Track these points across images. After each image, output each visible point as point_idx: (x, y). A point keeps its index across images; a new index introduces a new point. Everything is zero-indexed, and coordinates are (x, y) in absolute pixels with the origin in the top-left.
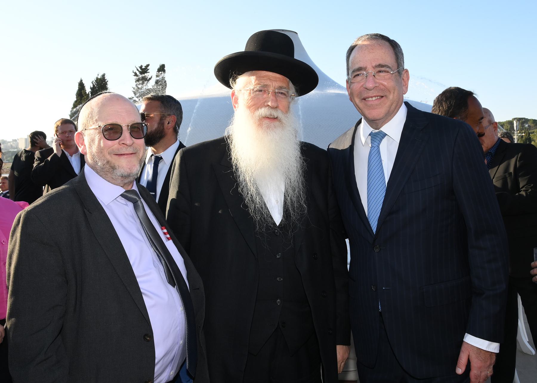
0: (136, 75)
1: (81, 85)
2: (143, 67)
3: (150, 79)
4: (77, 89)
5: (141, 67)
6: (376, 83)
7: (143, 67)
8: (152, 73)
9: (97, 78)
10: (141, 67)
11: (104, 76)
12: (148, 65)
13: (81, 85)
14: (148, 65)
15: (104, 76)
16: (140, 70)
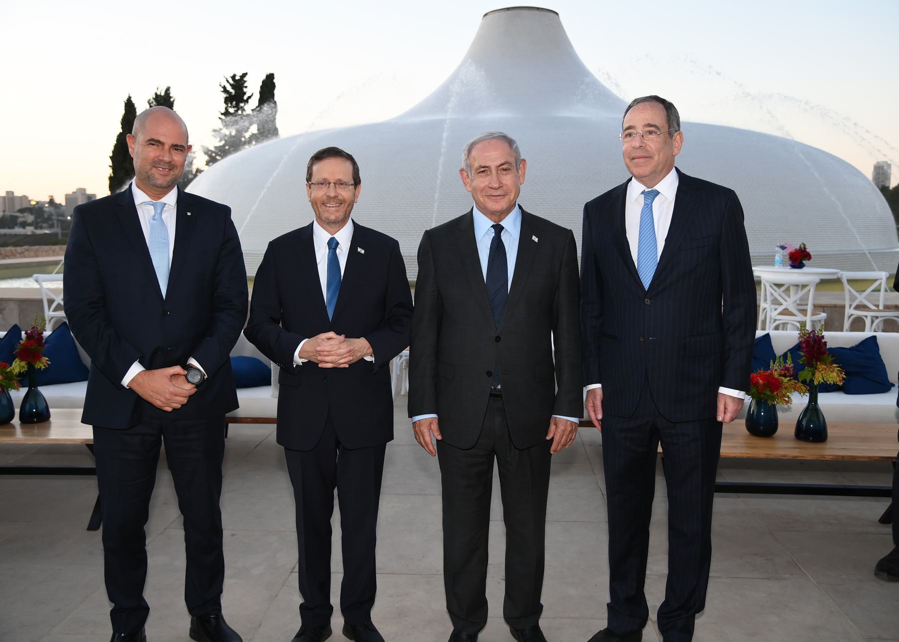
0: (225, 90)
1: (130, 106)
2: (237, 78)
3: (249, 97)
4: (123, 112)
5: (233, 77)
6: (642, 142)
7: (237, 78)
8: (253, 88)
9: (156, 94)
10: (233, 77)
11: (168, 89)
12: (245, 75)
13: (130, 106)
14: (245, 75)
15: (168, 89)
16: (232, 82)
